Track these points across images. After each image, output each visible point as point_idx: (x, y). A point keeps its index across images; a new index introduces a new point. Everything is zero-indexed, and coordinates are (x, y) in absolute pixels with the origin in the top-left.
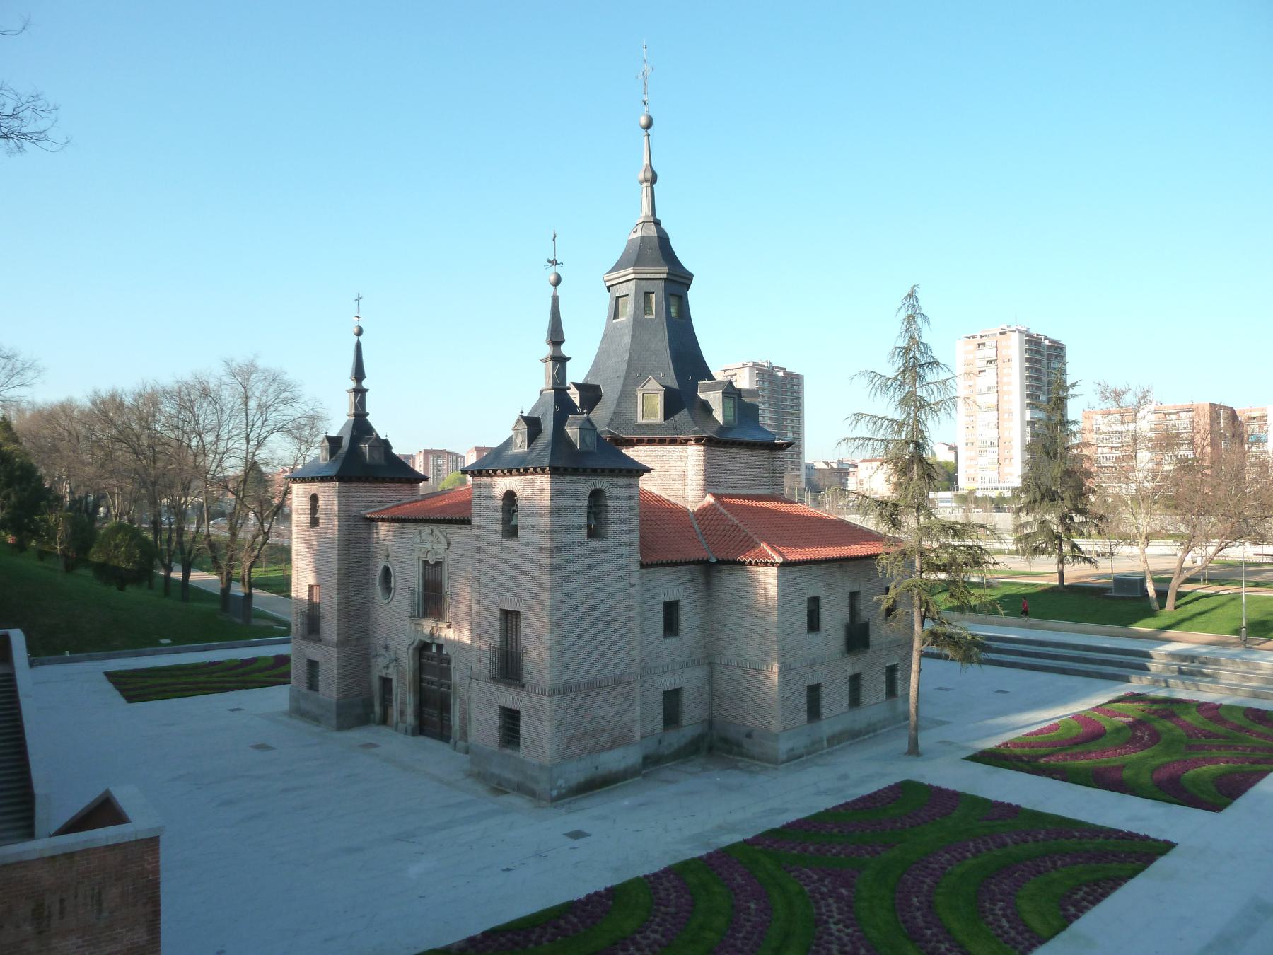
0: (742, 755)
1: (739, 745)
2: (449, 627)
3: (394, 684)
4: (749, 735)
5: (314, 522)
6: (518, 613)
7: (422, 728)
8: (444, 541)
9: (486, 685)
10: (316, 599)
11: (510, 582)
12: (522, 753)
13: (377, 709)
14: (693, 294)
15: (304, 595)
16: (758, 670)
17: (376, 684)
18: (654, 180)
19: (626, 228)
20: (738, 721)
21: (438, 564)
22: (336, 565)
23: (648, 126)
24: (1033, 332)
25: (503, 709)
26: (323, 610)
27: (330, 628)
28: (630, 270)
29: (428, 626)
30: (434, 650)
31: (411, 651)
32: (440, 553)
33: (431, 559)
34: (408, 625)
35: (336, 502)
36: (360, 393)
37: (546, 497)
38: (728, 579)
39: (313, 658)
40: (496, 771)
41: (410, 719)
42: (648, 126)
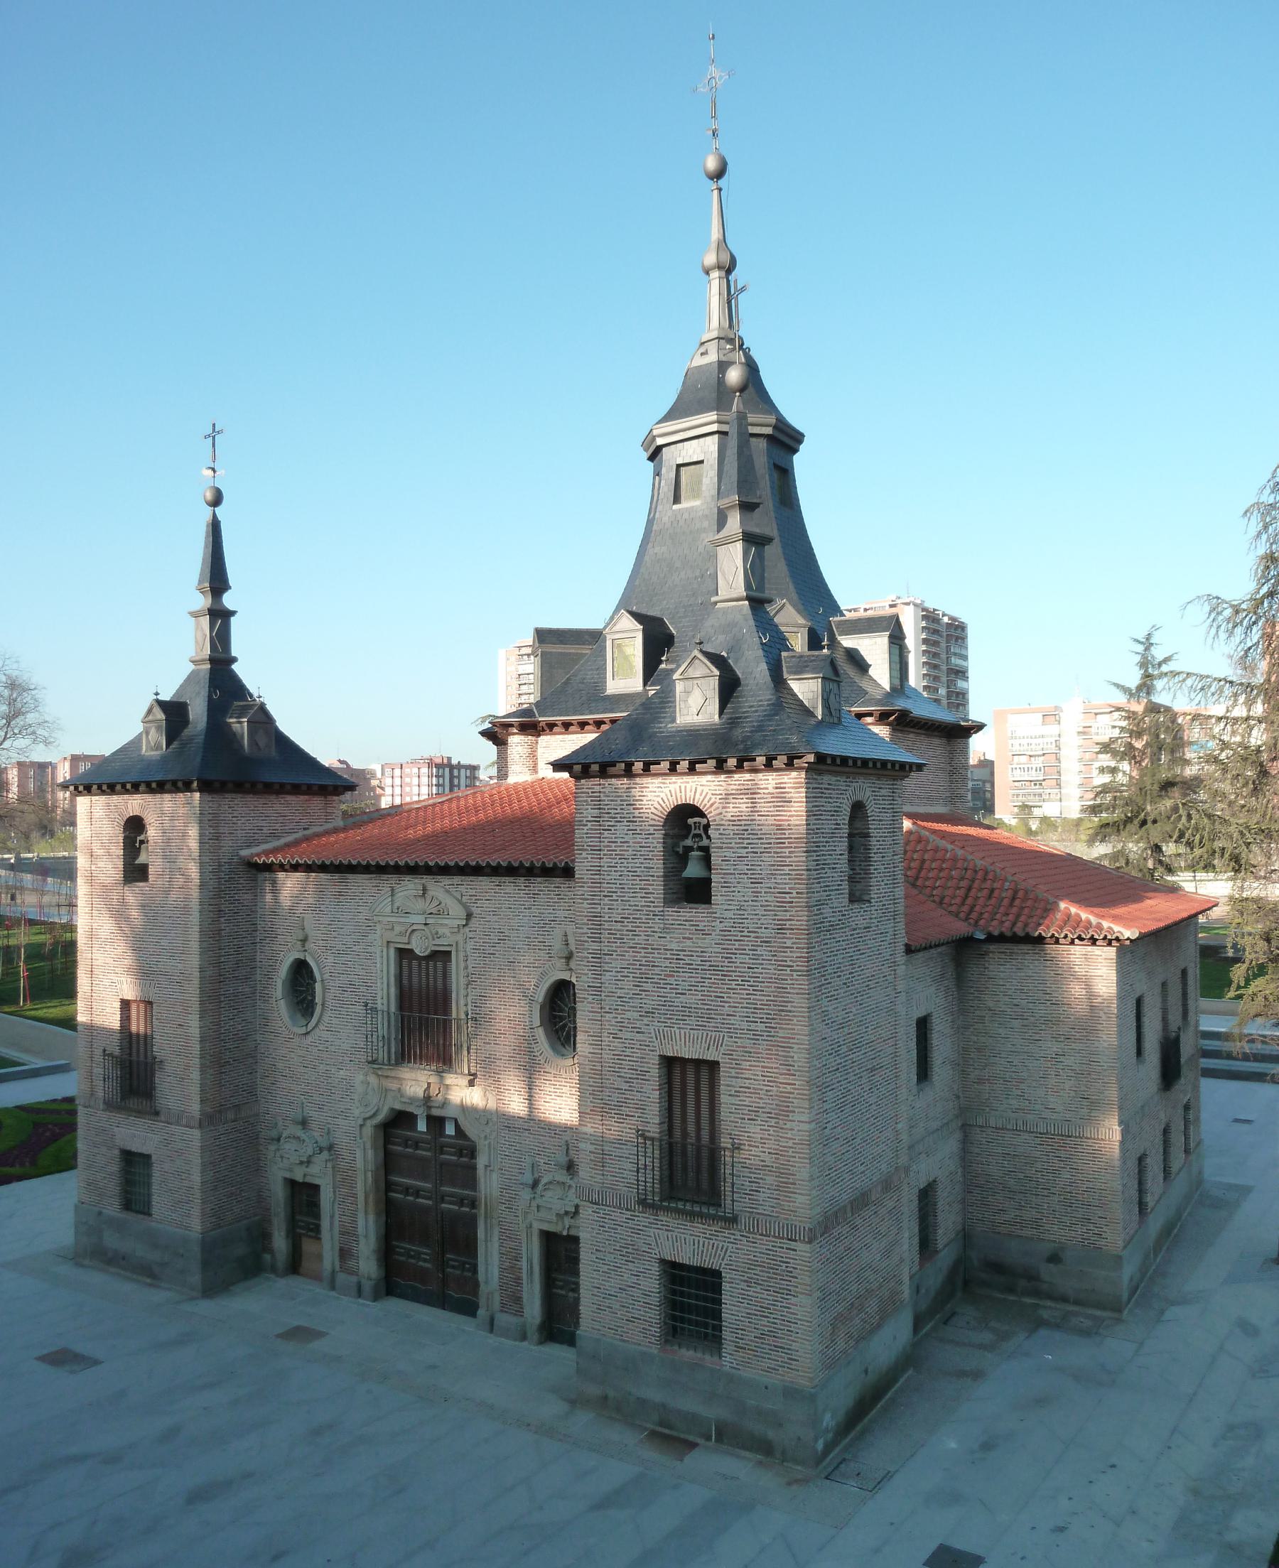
0: (1037, 1293)
1: (1032, 1276)
2: (471, 1083)
3: (326, 1197)
4: (1054, 1258)
5: (135, 872)
6: (713, 1066)
7: (394, 1281)
8: (457, 911)
9: (620, 1216)
10: (137, 1026)
11: (689, 999)
12: (729, 1359)
13: (280, 1242)
14: (802, 463)
15: (111, 1018)
16: (1065, 1137)
17: (278, 1194)
18: (728, 268)
19: (689, 347)
20: (1027, 1232)
21: (442, 956)
22: (194, 961)
23: (719, 174)
24: (930, 605)
25: (663, 1262)
26: (161, 1048)
27: (182, 1084)
28: (712, 416)
29: (415, 1082)
30: (422, 1126)
31: (368, 1131)
32: (446, 934)
33: (420, 947)
34: (361, 1079)
35: (193, 832)
36: (220, 617)
37: (796, 813)
38: (1004, 973)
39: (135, 1147)
40: (654, 1395)
41: (368, 1265)
42: (719, 174)
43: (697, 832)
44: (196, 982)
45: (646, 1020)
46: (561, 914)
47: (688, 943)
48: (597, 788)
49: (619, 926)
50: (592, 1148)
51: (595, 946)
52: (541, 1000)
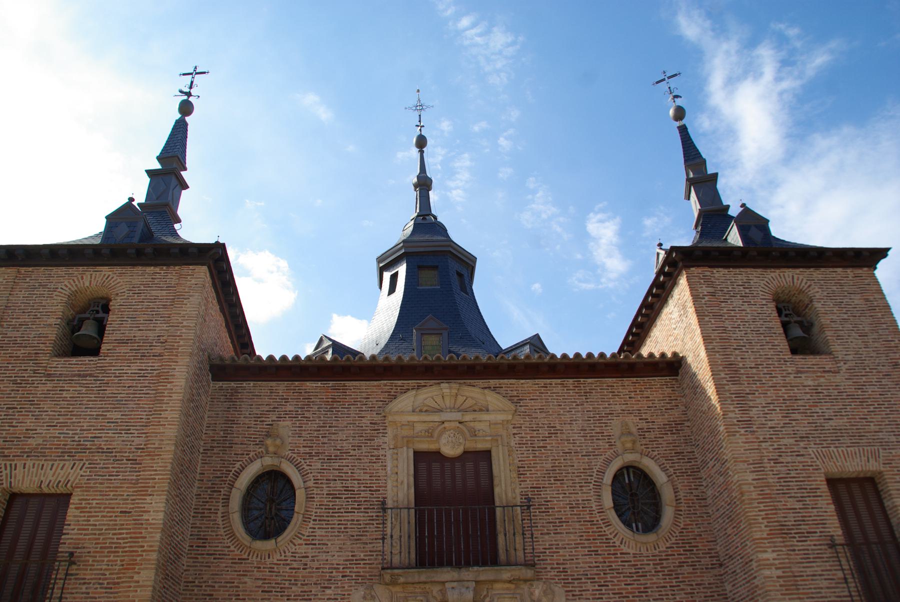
43: (787, 312)
44: (168, 457)
45: (802, 444)
46: (618, 408)
47: (822, 380)
48: (708, 273)
49: (754, 371)
50: (779, 573)
51: (734, 388)
52: (609, 482)
